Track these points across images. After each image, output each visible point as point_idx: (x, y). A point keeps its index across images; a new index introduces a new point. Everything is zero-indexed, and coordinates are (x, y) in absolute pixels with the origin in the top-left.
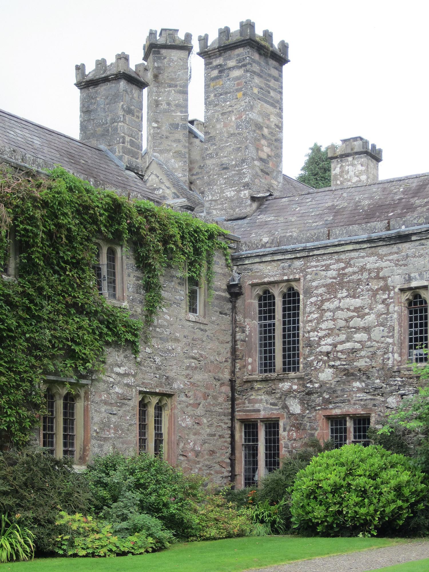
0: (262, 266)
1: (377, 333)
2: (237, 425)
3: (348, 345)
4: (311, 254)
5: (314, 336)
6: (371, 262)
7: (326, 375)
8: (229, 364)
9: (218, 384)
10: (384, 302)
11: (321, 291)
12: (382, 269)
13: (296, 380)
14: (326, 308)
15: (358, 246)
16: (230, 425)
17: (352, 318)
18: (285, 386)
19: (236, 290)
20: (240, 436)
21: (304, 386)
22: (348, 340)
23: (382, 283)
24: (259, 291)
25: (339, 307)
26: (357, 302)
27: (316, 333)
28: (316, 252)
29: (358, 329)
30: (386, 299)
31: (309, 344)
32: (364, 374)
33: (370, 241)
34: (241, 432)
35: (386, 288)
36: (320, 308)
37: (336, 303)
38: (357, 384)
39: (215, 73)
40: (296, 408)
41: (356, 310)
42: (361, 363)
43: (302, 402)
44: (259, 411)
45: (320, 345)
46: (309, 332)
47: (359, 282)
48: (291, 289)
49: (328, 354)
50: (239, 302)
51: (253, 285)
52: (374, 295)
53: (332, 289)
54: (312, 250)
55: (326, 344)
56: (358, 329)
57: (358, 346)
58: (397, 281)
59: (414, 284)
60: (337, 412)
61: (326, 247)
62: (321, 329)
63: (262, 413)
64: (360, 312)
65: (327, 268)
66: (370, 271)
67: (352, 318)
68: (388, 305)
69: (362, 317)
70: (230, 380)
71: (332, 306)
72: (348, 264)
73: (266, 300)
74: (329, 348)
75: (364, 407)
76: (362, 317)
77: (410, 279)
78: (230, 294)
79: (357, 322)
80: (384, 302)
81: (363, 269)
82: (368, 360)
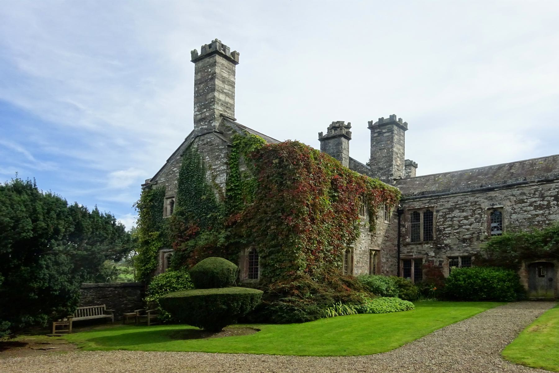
5: (441, 227)
6: (471, 199)
8: (397, 239)
11: (444, 211)
17: (462, 220)
21: (436, 246)
26: (465, 214)
33: (471, 191)
50: (402, 216)
54: (441, 196)
58: (486, 205)
64: (466, 218)
67: (462, 220)
68: (481, 215)
73: (416, 214)
77: (493, 205)
80: (479, 214)
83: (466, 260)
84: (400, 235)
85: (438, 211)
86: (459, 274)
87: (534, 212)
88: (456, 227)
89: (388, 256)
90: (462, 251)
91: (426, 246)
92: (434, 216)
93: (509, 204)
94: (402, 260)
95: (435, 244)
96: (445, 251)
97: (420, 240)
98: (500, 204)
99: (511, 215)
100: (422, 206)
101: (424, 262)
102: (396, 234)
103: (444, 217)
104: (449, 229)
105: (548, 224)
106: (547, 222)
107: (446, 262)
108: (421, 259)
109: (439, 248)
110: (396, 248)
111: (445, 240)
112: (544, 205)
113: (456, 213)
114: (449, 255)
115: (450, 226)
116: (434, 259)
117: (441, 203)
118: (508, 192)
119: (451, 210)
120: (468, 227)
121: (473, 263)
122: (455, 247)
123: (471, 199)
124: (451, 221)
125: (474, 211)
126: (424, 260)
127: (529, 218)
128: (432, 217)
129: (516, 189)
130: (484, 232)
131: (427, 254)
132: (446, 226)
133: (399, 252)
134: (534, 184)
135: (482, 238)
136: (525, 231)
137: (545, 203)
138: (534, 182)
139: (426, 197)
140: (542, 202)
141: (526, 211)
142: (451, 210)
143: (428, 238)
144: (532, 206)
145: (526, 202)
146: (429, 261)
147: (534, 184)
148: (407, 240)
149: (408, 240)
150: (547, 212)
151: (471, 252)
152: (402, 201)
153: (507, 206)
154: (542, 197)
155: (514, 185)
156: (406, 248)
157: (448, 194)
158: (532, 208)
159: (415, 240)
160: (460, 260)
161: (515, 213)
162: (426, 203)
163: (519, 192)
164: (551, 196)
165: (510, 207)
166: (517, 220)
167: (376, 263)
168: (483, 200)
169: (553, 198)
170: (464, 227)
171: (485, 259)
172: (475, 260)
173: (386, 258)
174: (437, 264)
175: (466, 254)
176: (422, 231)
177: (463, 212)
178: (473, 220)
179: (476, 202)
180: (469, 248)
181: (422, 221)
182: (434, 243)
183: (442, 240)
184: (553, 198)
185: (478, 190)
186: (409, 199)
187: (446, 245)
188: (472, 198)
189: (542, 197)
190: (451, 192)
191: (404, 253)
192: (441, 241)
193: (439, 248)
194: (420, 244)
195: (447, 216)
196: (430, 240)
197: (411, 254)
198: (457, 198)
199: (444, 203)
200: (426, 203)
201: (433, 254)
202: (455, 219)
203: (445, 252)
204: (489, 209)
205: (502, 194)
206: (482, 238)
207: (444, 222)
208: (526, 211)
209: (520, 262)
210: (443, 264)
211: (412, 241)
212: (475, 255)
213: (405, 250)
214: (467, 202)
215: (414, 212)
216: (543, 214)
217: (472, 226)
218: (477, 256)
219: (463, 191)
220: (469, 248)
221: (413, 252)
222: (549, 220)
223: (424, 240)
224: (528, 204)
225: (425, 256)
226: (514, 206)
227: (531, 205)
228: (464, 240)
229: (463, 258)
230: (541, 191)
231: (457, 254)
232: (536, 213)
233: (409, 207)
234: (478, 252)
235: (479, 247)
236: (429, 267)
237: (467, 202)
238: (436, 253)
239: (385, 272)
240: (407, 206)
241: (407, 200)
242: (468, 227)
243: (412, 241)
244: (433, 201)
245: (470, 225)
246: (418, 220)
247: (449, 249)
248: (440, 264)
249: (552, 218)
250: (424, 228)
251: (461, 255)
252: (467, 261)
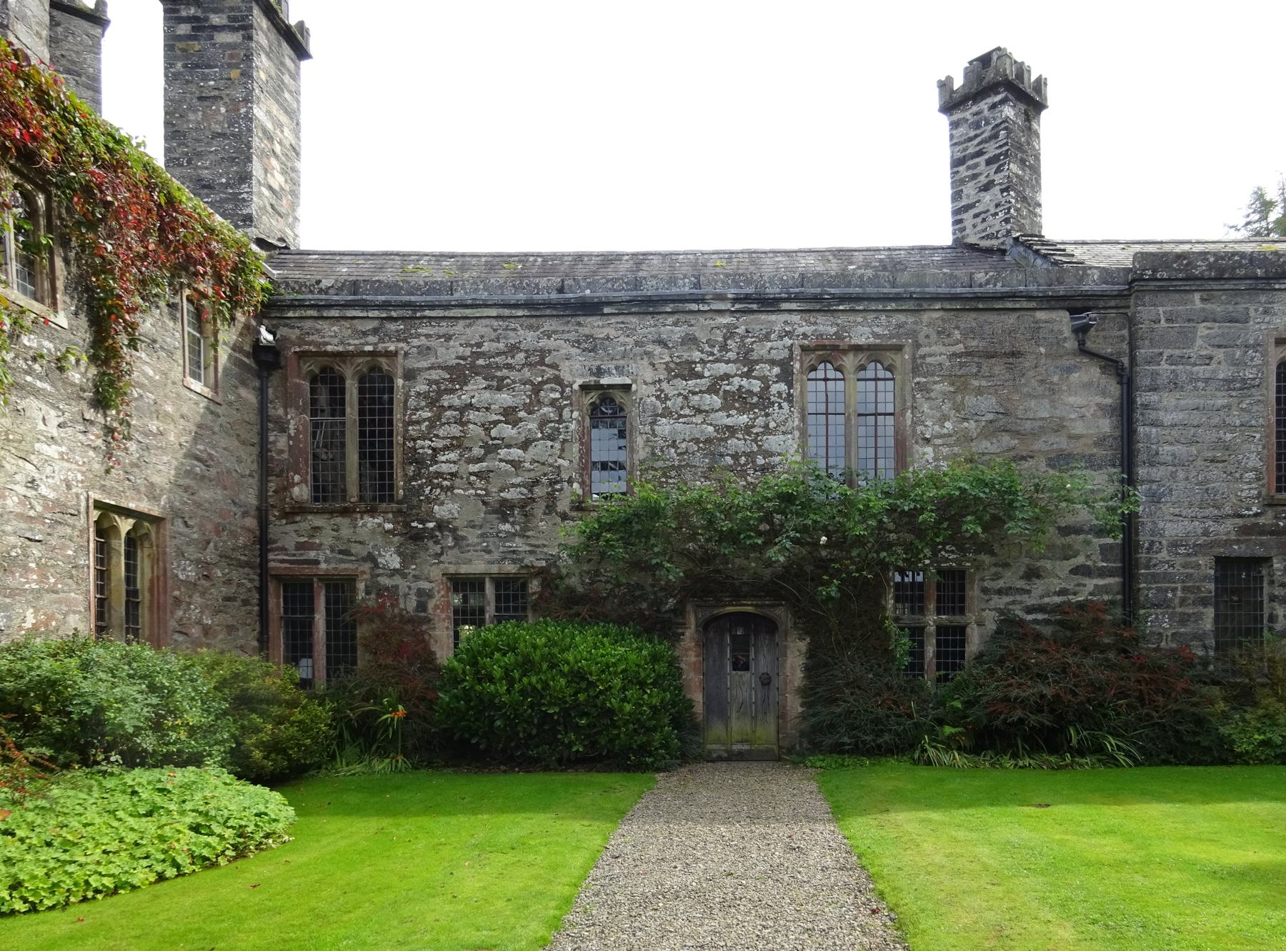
0: (320, 325)
2: (271, 587)
4: (418, 315)
5: (424, 446)
6: (528, 338)
8: (254, 482)
9: (239, 512)
11: (435, 375)
12: (550, 351)
13: (390, 516)
14: (446, 404)
15: (506, 312)
16: (257, 584)
17: (496, 423)
19: (270, 358)
20: (276, 604)
24: (310, 366)
25: (471, 404)
26: (505, 398)
27: (428, 443)
28: (427, 313)
30: (557, 400)
33: (528, 305)
34: (278, 598)
36: (433, 401)
44: (317, 562)
45: (436, 462)
46: (415, 440)
48: (375, 368)
51: (302, 355)
54: (422, 307)
55: (448, 461)
58: (575, 371)
61: (448, 306)
62: (437, 436)
63: (323, 566)
64: (509, 415)
67: (496, 423)
68: (560, 410)
70: (259, 509)
76: (515, 423)
77: (599, 372)
78: (257, 362)
80: (553, 403)
82: (525, 491)
83: (511, 591)
84: (266, 465)
85: (410, 375)
86: (488, 649)
87: (722, 419)
88: (477, 452)
89: (210, 555)
90: (496, 556)
91: (371, 522)
92: (398, 396)
93: (649, 375)
94: (278, 578)
95: (403, 516)
96: (438, 549)
97: (344, 499)
98: (620, 370)
99: (653, 423)
100: (353, 344)
101: (361, 595)
102: (249, 462)
103: (433, 401)
104: (453, 456)
105: (764, 469)
106: (760, 461)
107: (443, 602)
108: (351, 580)
109: (417, 537)
110: (251, 522)
111: (436, 501)
112: (750, 392)
113: (475, 391)
114: (452, 569)
115: (457, 444)
116: (397, 580)
117: (423, 340)
118: (645, 327)
119: (459, 375)
120: (516, 453)
121: (535, 608)
122: (472, 536)
123: (528, 338)
124: (460, 422)
125: (537, 389)
126: (361, 586)
127: (709, 441)
128: (391, 401)
129: (670, 320)
130: (570, 482)
131: (371, 558)
132: (439, 444)
133: (263, 541)
134: (722, 306)
135: (563, 505)
136: (699, 486)
137: (756, 386)
138: (721, 298)
139: (364, 305)
140: (744, 382)
141: (698, 411)
142: (459, 375)
143: (379, 490)
144: (717, 393)
145: (701, 376)
146: (381, 591)
147: (722, 306)
148: (296, 490)
149: (301, 492)
150: (760, 421)
151: (529, 560)
152: (272, 309)
153: (643, 379)
154: (748, 361)
155: (665, 300)
156: (290, 528)
157: (448, 306)
158: (717, 401)
159: (327, 494)
160: (489, 589)
161: (667, 413)
162: (365, 334)
163: (679, 332)
164: (773, 363)
165: (652, 390)
166: (674, 444)
167: (143, 582)
168: (567, 349)
169: (776, 370)
170: (503, 452)
171: (571, 590)
172: (541, 595)
173: (198, 562)
174: (411, 604)
175: (510, 568)
176: (353, 456)
177: (499, 389)
178: (533, 426)
179: (543, 353)
180: (519, 544)
181: (352, 412)
182: (400, 512)
183: (429, 500)
184: (776, 370)
185: (549, 304)
186: (300, 305)
187: (442, 525)
188: (530, 335)
189: (748, 361)
190: (457, 295)
191: (283, 549)
192: (424, 507)
193: (417, 537)
194: (345, 512)
195: (446, 400)
196: (382, 499)
197: (312, 554)
198: (480, 329)
199: (433, 343)
200: (365, 334)
201: (395, 562)
202: (472, 415)
203: (438, 555)
204: (585, 388)
205: (629, 332)
206: (563, 505)
207: (434, 422)
208: (698, 411)
209: (679, 611)
210: (431, 605)
211: (316, 499)
212: (541, 572)
213: (287, 535)
214: (513, 349)
215: (323, 370)
216: (748, 429)
217: (532, 451)
218: (548, 576)
219: (497, 298)
220: (519, 544)
221: (319, 547)
222: (768, 454)
223: (361, 498)
224: (704, 383)
225: (367, 566)
226: (664, 385)
227: (712, 390)
228: (503, 510)
229: (502, 582)
230: (743, 338)
231: (477, 566)
232: (729, 421)
233: (301, 341)
234: (553, 561)
235: (556, 539)
236: (381, 617)
237: (513, 349)
238: (406, 558)
239: (195, 631)
240: (293, 334)
241: (294, 305)
242: (516, 453)
243: (316, 499)
244: (392, 327)
245: (525, 445)
246: (338, 405)
247: (450, 542)
248: (422, 606)
249: (775, 448)
250: (362, 445)
251: (494, 569)
252: (516, 598)
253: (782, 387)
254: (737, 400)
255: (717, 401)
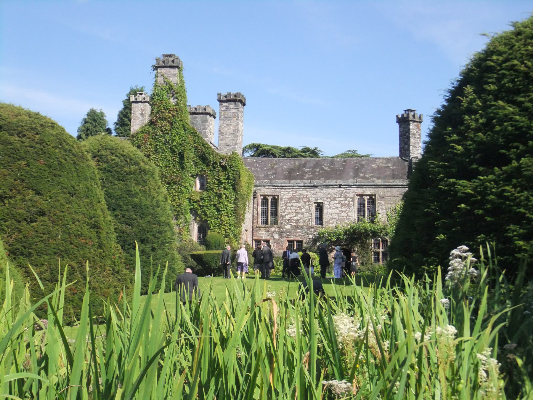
1: (306, 215)
3: (296, 218)
5: (283, 214)
7: (288, 227)
10: (308, 205)
18: (273, 229)
22: (295, 216)
23: (308, 200)
26: (299, 205)
29: (299, 213)
31: (282, 216)
32: (302, 227)
35: (309, 201)
37: (292, 204)
38: (299, 230)
39: (224, 108)
40: (277, 236)
41: (298, 207)
42: (301, 224)
43: (279, 235)
47: (300, 198)
49: (288, 220)
52: (305, 203)
53: (290, 199)
56: (299, 213)
57: (299, 218)
58: (313, 199)
59: (319, 201)
60: (292, 239)
65: (289, 192)
66: (304, 195)
69: (301, 209)
71: (290, 205)
72: (296, 192)
74: (289, 218)
75: (301, 238)
77: (317, 200)
79: (299, 211)
80: (308, 205)
81: (301, 194)
87: (340, 209)
132: (286, 213)
137: (347, 202)
154: (346, 198)
179: (307, 195)
216: (345, 211)
227: (339, 203)
253: (352, 203)
254: (343, 205)
255: (340, 205)
